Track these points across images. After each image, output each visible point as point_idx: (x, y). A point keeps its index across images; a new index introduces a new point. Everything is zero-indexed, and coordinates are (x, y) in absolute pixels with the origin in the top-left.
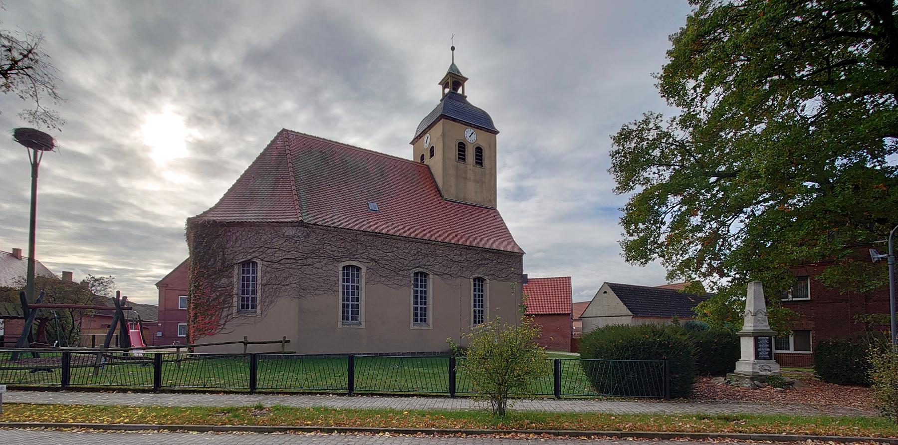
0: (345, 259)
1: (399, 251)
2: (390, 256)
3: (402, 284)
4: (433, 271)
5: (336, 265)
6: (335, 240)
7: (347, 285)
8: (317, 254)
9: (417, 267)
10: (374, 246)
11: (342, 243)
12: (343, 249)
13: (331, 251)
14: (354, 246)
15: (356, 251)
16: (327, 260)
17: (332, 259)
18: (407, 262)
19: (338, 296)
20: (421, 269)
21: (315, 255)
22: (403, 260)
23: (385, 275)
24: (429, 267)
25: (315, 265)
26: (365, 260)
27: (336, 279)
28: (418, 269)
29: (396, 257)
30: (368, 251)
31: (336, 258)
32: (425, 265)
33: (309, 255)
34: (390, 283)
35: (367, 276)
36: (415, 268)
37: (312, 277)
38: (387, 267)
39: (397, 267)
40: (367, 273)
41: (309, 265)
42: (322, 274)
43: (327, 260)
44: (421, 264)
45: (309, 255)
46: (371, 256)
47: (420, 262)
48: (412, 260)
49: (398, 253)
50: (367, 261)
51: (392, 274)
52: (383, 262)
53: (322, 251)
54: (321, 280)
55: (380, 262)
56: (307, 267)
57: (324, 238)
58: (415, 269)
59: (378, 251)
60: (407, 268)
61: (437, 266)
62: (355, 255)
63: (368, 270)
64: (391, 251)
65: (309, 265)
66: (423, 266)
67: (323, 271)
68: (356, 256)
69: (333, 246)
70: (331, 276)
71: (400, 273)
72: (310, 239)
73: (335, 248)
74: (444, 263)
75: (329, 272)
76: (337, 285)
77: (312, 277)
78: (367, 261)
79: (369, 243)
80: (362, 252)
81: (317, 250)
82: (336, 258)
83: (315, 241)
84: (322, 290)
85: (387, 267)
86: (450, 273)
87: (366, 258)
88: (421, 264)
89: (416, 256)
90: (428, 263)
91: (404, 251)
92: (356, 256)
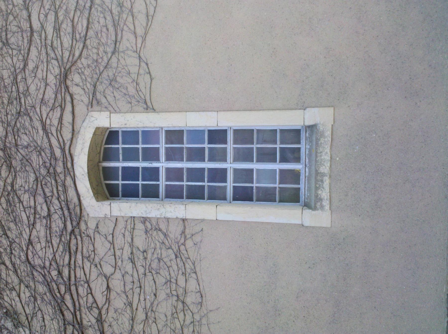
0: (71, 193)
5: (92, 225)
6: (12, 225)
7: (168, 179)
8: (63, 289)
10: (15, 82)
11: (21, 202)
12: (40, 199)
13: (49, 242)
14: (26, 160)
15: (40, 150)
16: (79, 256)
17: (73, 241)
19: (203, 220)
21: (68, 297)
23: (111, 29)
25: (101, 300)
26: (67, 117)
27: (140, 226)
30: (33, 107)
31: (69, 228)
33: (69, 316)
35: (122, 104)
37: (141, 316)
40: (114, 110)
41: (100, 320)
42: (128, 279)
43: (79, 256)
45: (69, 316)
46: (50, 94)
50: (69, 108)
52: (67, 41)
53: (54, 273)
54: (148, 286)
55: (66, 54)
56: (106, 325)
57: (13, 265)
59: (31, 65)
62: (52, 153)
63: (98, 103)
65: (100, 320)
67: (118, 275)
68: (58, 153)
69: (34, 233)
70: (131, 245)
72: (19, 308)
73: (38, 226)
75: (118, 253)
76: (163, 227)
77: (141, 316)
78: (69, 108)
79: (10, 103)
80: (41, 132)
81: (51, 291)
82: (69, 228)
83: (26, 294)
84: (182, 282)
85: (81, 27)
87: (57, 113)
92: (58, 153)
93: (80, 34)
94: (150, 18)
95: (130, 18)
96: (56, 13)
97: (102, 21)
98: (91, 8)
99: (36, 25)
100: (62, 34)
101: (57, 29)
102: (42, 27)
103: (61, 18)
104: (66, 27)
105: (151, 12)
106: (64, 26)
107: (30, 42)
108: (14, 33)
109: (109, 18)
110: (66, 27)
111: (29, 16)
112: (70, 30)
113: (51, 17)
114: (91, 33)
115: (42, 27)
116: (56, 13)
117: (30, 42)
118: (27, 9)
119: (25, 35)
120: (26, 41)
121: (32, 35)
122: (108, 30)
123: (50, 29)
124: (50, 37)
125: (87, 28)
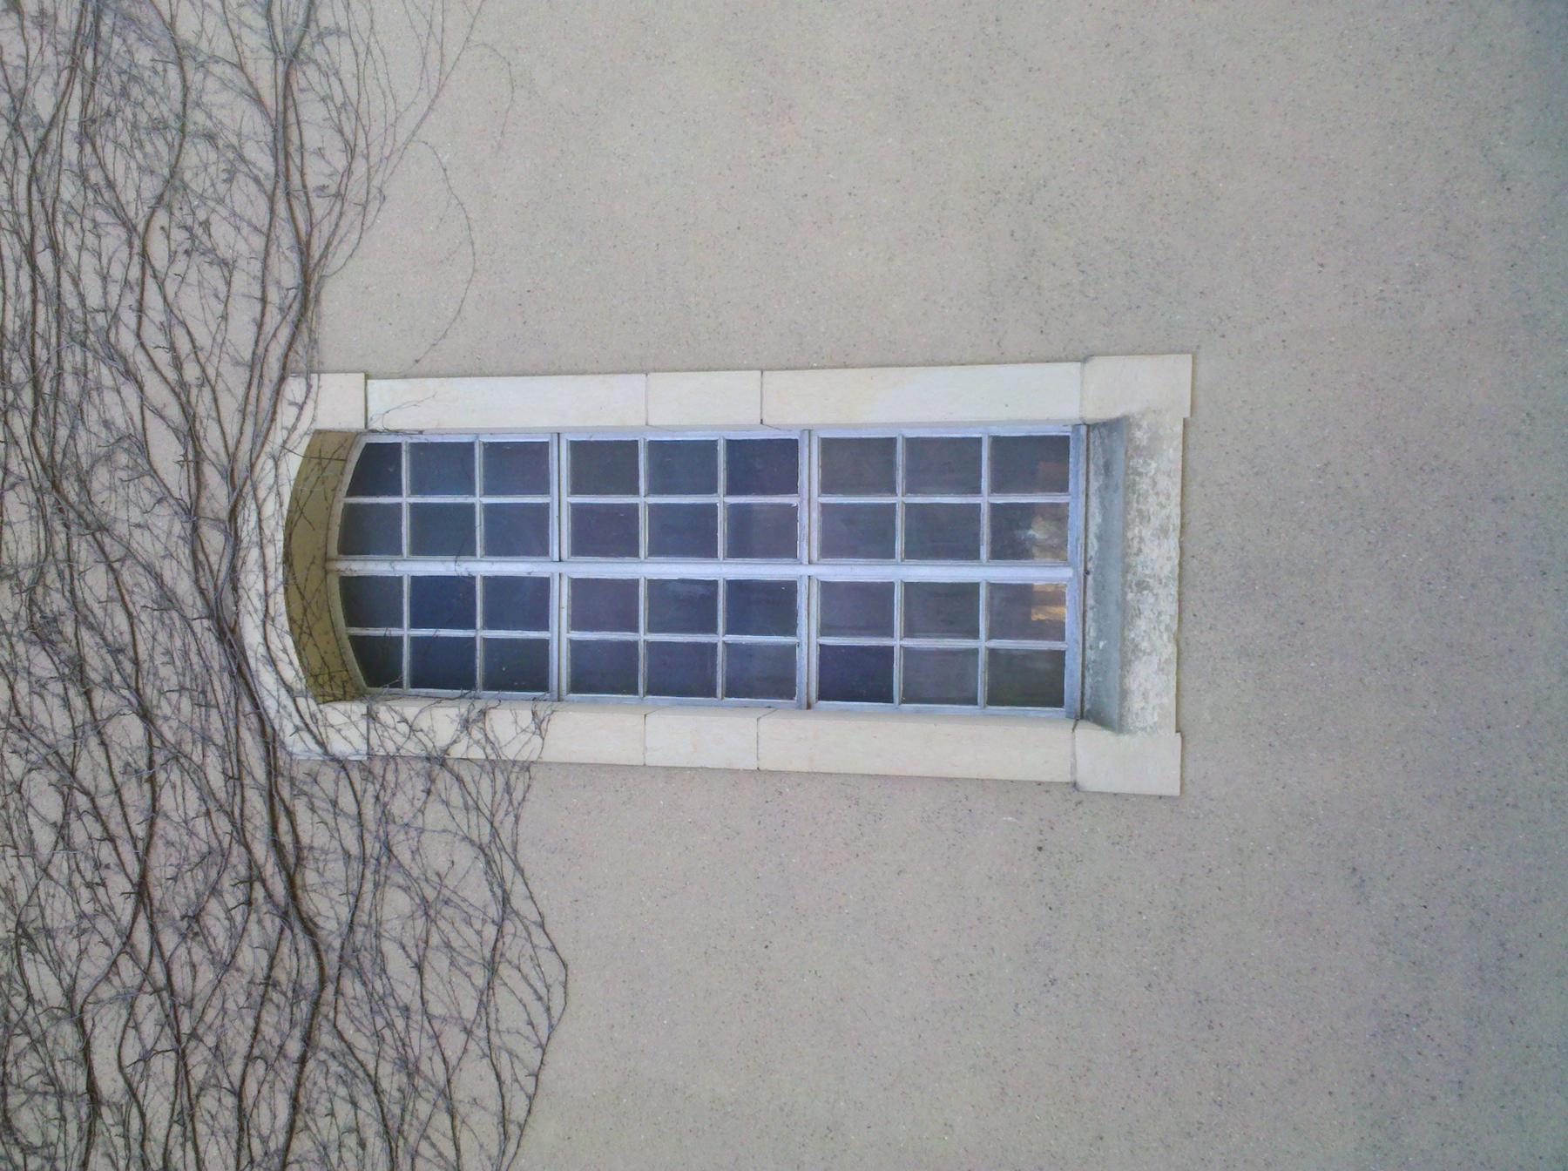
1: (59, 911)
2: (131, 1053)
3: (477, 892)
4: (256, 364)
9: (228, 635)
18: (179, 799)
20: (252, 580)
22: (162, 862)
23: (376, 1145)
24: (212, 441)
28: (251, 635)
29: (127, 968)
32: (192, 513)
34: (474, 1081)
36: (240, 673)
38: (271, 1115)
39: (251, 959)
44: (184, 587)
47: (167, 600)
48: (146, 715)
49: (83, 925)
51: (363, 1044)
58: (266, 678)
60: (256, 803)
61: (189, 303)
64: (68, 1030)
66: (214, 540)
71: (328, 909)
74: (136, 189)
85: (271, 1115)
86: (265, 74)
88: (184, 587)
89: (96, 662)
90: (166, 450)
91: (45, 838)
93: (265, 1141)
94: (513, 1129)
95: (443, 1120)
96: (182, 1056)
97: (344, 1111)
98: (303, 1060)
99: (110, 1083)
100: (201, 1128)
101: (185, 1116)
102: (132, 1091)
103: (198, 1073)
104: (216, 1107)
105: (518, 1110)
106: (208, 1102)
107: (89, 1136)
108: (31, 1093)
109: (368, 1104)
110: (216, 1107)
111: (86, 1051)
112: (228, 1120)
113: (164, 1066)
114: (302, 1144)
115: (132, 1091)
116: (182, 1056)
117: (89, 1136)
118: (80, 1024)
119: (69, 1109)
120: (72, 1127)
121: (95, 1114)
122: (362, 1144)
123: (159, 1105)
124: (158, 1131)
125: (291, 1130)
